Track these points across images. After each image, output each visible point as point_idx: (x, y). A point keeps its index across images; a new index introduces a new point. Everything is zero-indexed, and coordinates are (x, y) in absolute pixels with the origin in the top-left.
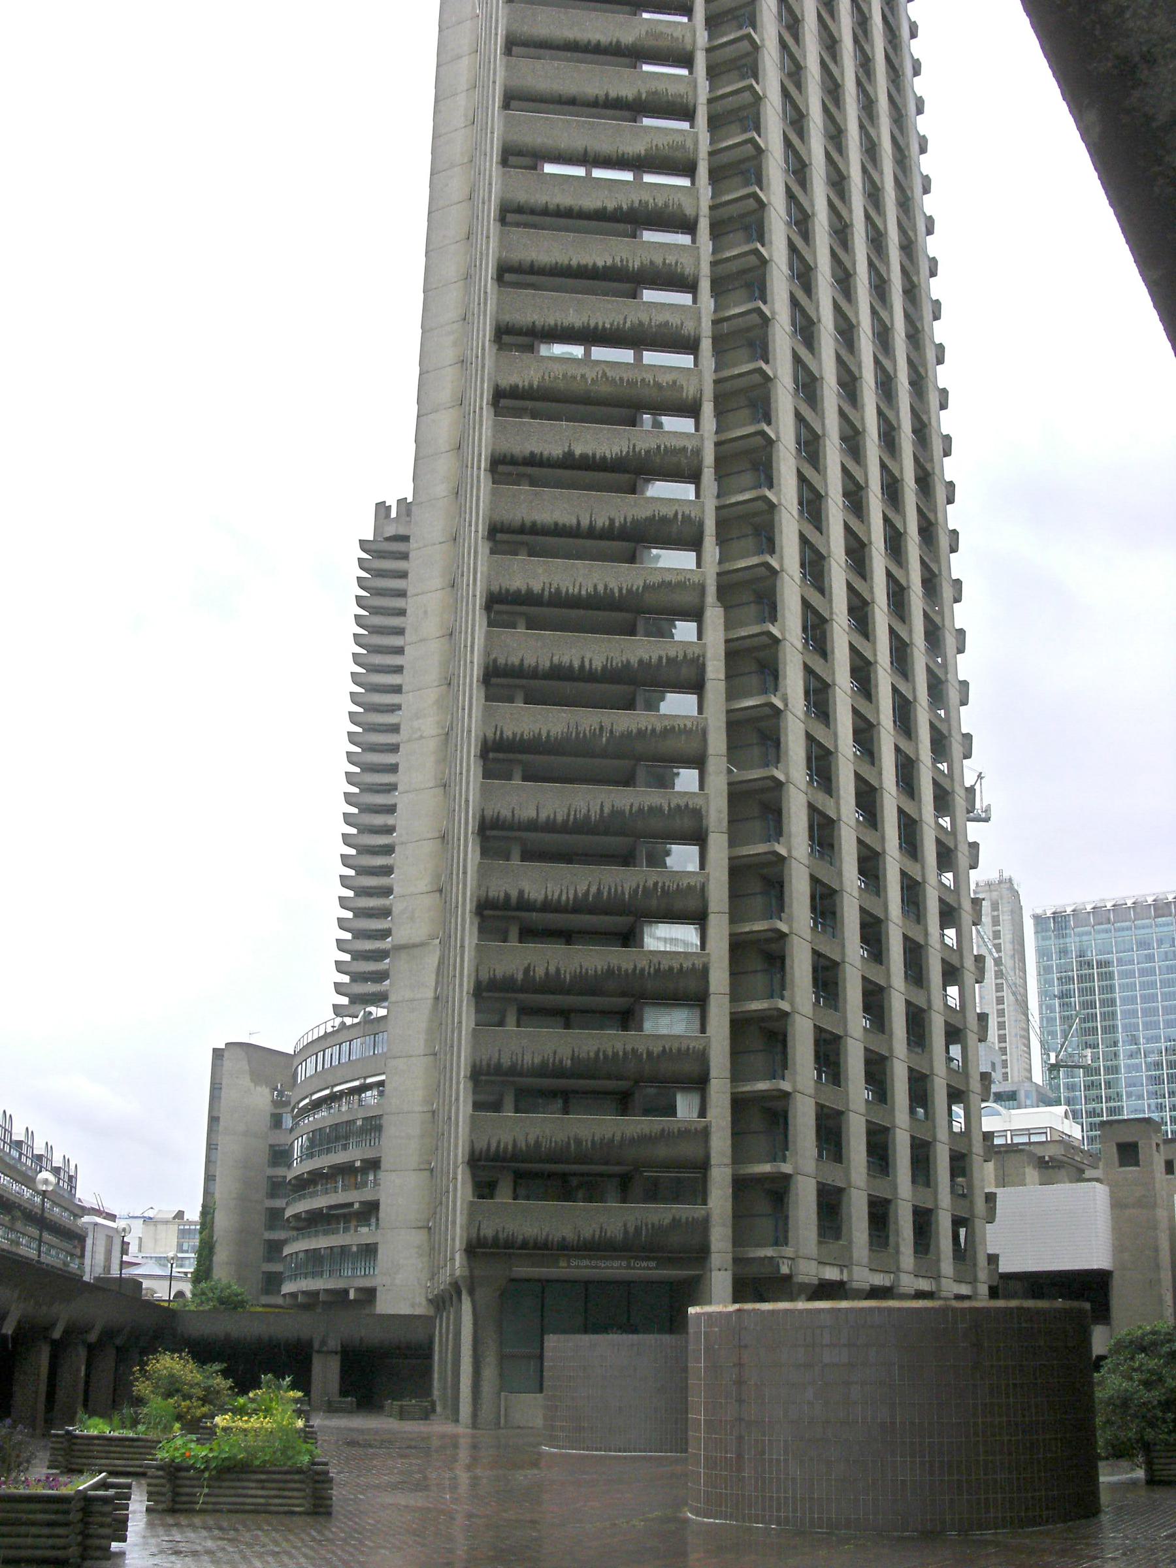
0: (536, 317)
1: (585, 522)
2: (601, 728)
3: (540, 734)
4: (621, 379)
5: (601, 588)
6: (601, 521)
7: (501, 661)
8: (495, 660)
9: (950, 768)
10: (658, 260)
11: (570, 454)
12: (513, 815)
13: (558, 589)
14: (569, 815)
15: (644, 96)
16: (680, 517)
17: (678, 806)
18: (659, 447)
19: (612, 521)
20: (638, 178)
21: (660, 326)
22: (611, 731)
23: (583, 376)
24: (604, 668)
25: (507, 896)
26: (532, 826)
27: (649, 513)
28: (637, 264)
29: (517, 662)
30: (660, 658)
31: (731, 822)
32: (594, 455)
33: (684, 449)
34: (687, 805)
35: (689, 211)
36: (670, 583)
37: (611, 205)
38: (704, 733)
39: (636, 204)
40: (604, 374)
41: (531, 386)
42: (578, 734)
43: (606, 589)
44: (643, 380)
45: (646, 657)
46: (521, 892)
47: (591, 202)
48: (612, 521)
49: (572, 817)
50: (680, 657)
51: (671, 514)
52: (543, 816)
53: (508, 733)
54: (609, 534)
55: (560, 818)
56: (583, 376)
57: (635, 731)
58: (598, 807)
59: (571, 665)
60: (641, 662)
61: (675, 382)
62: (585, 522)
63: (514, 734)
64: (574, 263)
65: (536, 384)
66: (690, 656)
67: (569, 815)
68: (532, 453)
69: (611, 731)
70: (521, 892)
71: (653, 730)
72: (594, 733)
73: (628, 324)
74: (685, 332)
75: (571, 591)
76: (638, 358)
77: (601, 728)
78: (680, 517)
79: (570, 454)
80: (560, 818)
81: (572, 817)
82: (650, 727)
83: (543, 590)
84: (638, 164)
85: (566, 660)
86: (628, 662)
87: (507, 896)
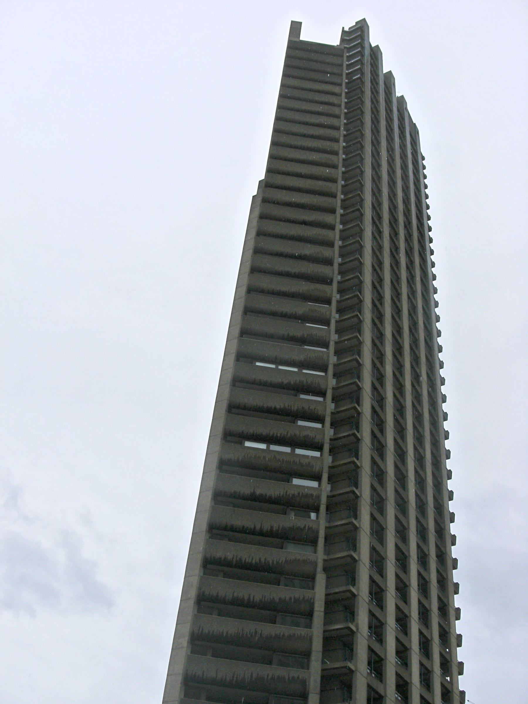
1: (258, 527)
2: (256, 633)
3: (223, 632)
4: (283, 460)
5: (263, 560)
6: (266, 527)
7: (207, 593)
8: (204, 592)
9: (451, 679)
10: (306, 408)
12: (203, 675)
13: (240, 559)
14: (233, 677)
15: (305, 336)
16: (307, 528)
17: (293, 677)
18: (299, 493)
19: (272, 527)
21: (305, 437)
22: (261, 634)
23: (264, 457)
26: (214, 682)
29: (215, 594)
30: (291, 598)
31: (322, 691)
32: (266, 495)
33: (312, 495)
34: (298, 677)
35: (323, 387)
36: (299, 560)
37: (285, 382)
38: (311, 639)
39: (298, 382)
40: (275, 457)
42: (243, 634)
43: (265, 559)
44: (294, 461)
45: (283, 597)
47: (276, 379)
48: (272, 527)
49: (235, 679)
50: (301, 598)
51: (302, 526)
52: (219, 677)
53: (206, 631)
54: (271, 534)
55: (228, 679)
57: (273, 635)
58: (250, 674)
59: (243, 598)
60: (280, 599)
61: (309, 463)
62: (258, 527)
63: (209, 632)
64: (265, 406)
65: (240, 459)
66: (306, 598)
67: (233, 677)
69: (261, 634)
71: (284, 635)
72: (252, 634)
73: (289, 435)
74: (316, 440)
75: (247, 561)
76: (293, 451)
77: (256, 633)
78: (307, 528)
80: (228, 679)
81: (235, 679)
82: (282, 634)
83: (233, 558)
84: (302, 365)
85: (241, 595)
86: (273, 598)
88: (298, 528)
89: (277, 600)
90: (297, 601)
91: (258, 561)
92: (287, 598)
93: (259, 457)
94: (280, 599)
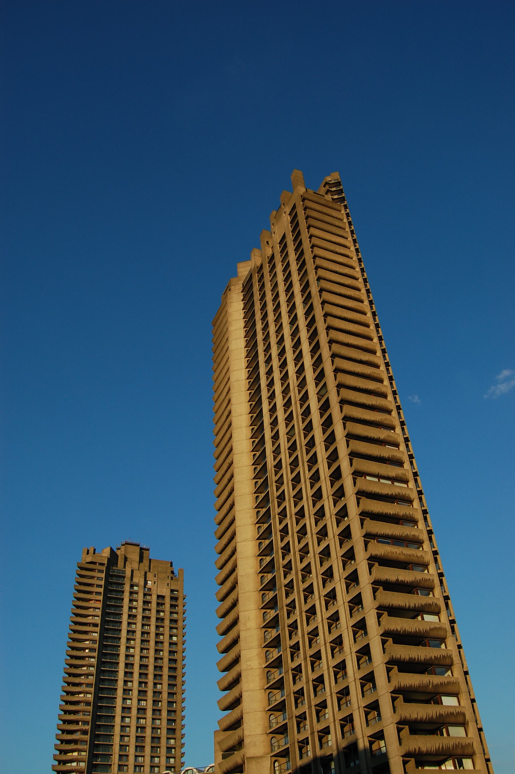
0: (378, 530)
2: (430, 682)
10: (408, 513)
11: (397, 580)
20: (393, 483)
21: (413, 535)
23: (396, 552)
24: (425, 659)
25: (415, 749)
27: (425, 602)
28: (402, 514)
30: (440, 656)
41: (381, 554)
45: (436, 655)
46: (419, 748)
48: (415, 605)
51: (431, 603)
53: (402, 685)
56: (396, 552)
60: (435, 657)
68: (387, 579)
70: (419, 748)
71: (445, 683)
74: (420, 538)
77: (430, 682)
79: (397, 580)
87: (415, 749)
88: (430, 604)
89: (433, 658)
90: (444, 657)
91: (415, 630)
92: (439, 656)
93: (393, 552)
94: (435, 657)
